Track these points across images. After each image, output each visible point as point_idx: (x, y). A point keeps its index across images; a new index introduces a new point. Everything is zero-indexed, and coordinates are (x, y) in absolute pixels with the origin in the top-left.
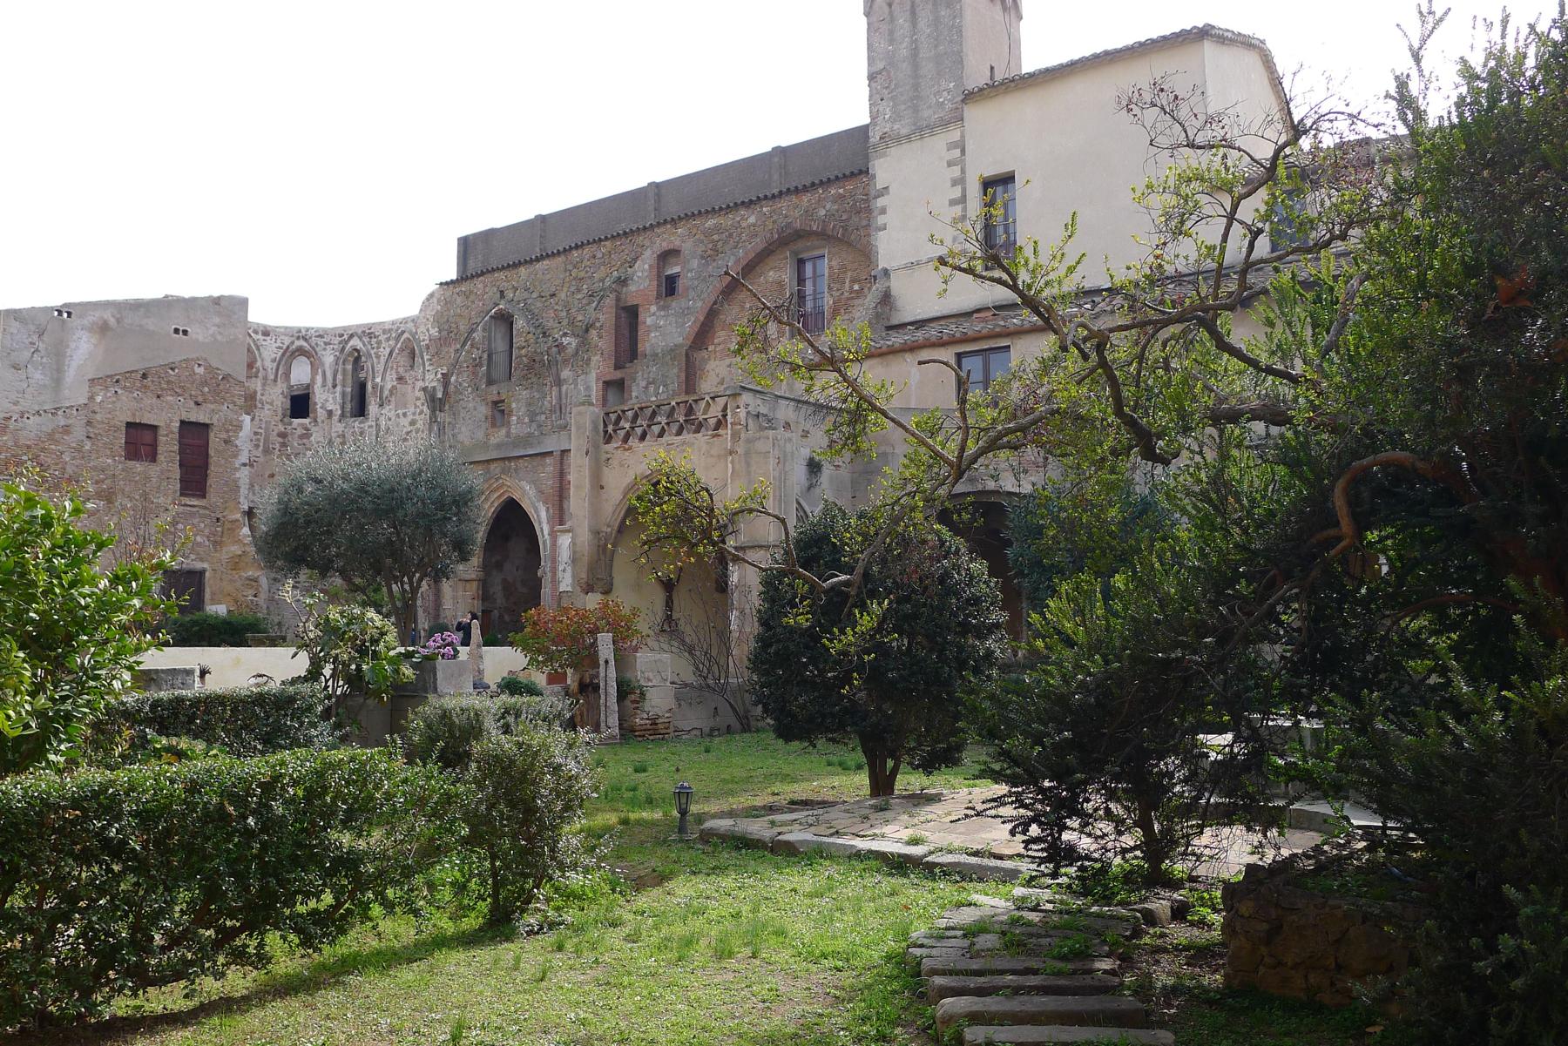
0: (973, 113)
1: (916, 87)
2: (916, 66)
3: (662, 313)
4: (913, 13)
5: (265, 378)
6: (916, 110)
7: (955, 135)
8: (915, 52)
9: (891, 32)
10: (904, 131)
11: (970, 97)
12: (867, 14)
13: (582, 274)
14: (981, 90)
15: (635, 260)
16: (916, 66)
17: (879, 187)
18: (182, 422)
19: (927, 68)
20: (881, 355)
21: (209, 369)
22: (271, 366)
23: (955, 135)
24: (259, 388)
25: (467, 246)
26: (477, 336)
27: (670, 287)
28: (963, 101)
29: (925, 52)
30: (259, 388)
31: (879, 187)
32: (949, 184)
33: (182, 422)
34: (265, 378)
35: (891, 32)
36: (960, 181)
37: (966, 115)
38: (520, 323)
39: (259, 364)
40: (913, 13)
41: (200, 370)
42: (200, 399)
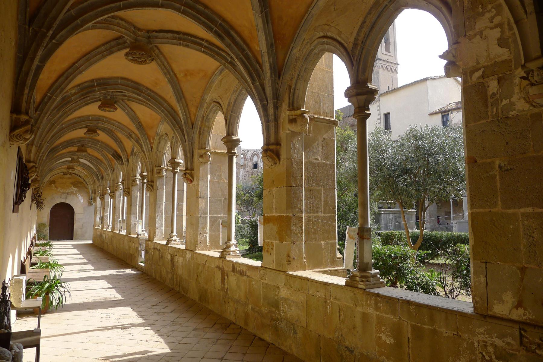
5: (248, 161)
7: (378, 104)
22: (249, 158)
23: (378, 104)
24: (247, 163)
30: (247, 163)
34: (248, 161)
36: (379, 114)
39: (247, 158)
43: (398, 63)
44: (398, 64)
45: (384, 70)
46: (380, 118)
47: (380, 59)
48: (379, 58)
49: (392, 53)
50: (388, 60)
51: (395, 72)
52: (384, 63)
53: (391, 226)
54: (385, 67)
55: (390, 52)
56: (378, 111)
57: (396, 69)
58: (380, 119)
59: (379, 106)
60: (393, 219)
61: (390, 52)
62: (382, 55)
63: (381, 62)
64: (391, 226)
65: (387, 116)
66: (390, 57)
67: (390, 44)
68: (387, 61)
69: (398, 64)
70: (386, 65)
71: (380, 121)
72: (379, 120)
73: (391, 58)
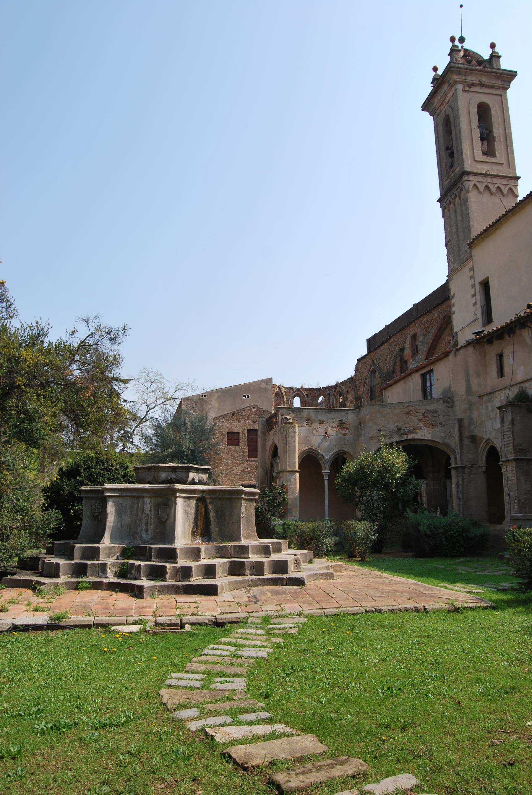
0: (477, 253)
1: (459, 245)
2: (458, 236)
3: (414, 362)
4: (456, 212)
6: (459, 256)
7: (471, 265)
8: (457, 231)
9: (450, 222)
10: (457, 267)
11: (472, 244)
12: (443, 217)
13: (392, 349)
14: (473, 242)
15: (405, 340)
16: (458, 236)
17: (452, 294)
18: (248, 430)
19: (461, 234)
20: (403, 378)
21: (258, 409)
23: (471, 265)
25: (369, 341)
26: (368, 380)
27: (415, 350)
28: (470, 248)
29: (460, 230)
31: (452, 294)
32: (471, 287)
33: (248, 430)
35: (450, 222)
36: (473, 286)
37: (473, 255)
38: (377, 374)
40: (456, 212)
41: (254, 410)
42: (255, 421)
43: (518, 175)
44: (519, 178)
45: (480, 193)
46: (475, 292)
47: (469, 173)
48: (467, 168)
49: (500, 156)
50: (488, 173)
51: (511, 196)
52: (480, 179)
53: (146, 530)
54: (482, 187)
55: (494, 156)
56: (471, 278)
57: (514, 189)
58: (474, 295)
59: (472, 269)
60: (151, 511)
61: (494, 156)
62: (476, 163)
63: (471, 178)
64: (146, 530)
65: (485, 285)
66: (495, 167)
67: (494, 139)
68: (486, 175)
69: (519, 178)
70: (485, 184)
71: (476, 299)
72: (474, 298)
73: (499, 167)
